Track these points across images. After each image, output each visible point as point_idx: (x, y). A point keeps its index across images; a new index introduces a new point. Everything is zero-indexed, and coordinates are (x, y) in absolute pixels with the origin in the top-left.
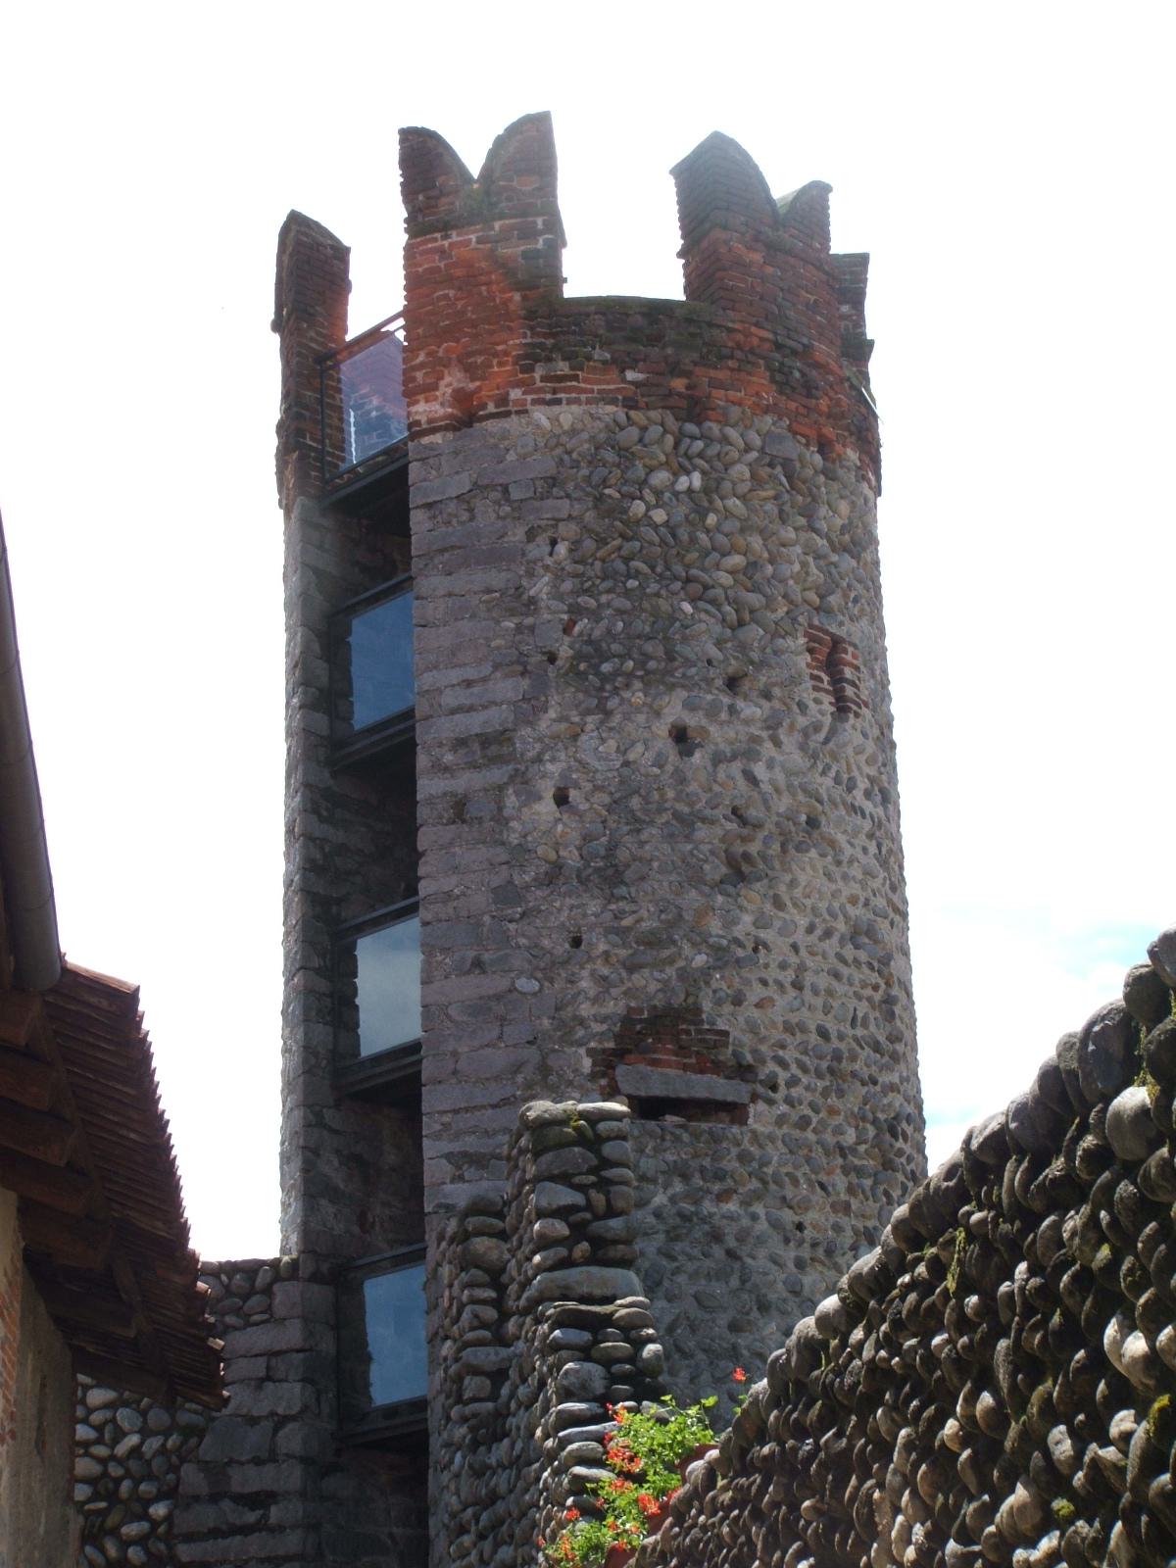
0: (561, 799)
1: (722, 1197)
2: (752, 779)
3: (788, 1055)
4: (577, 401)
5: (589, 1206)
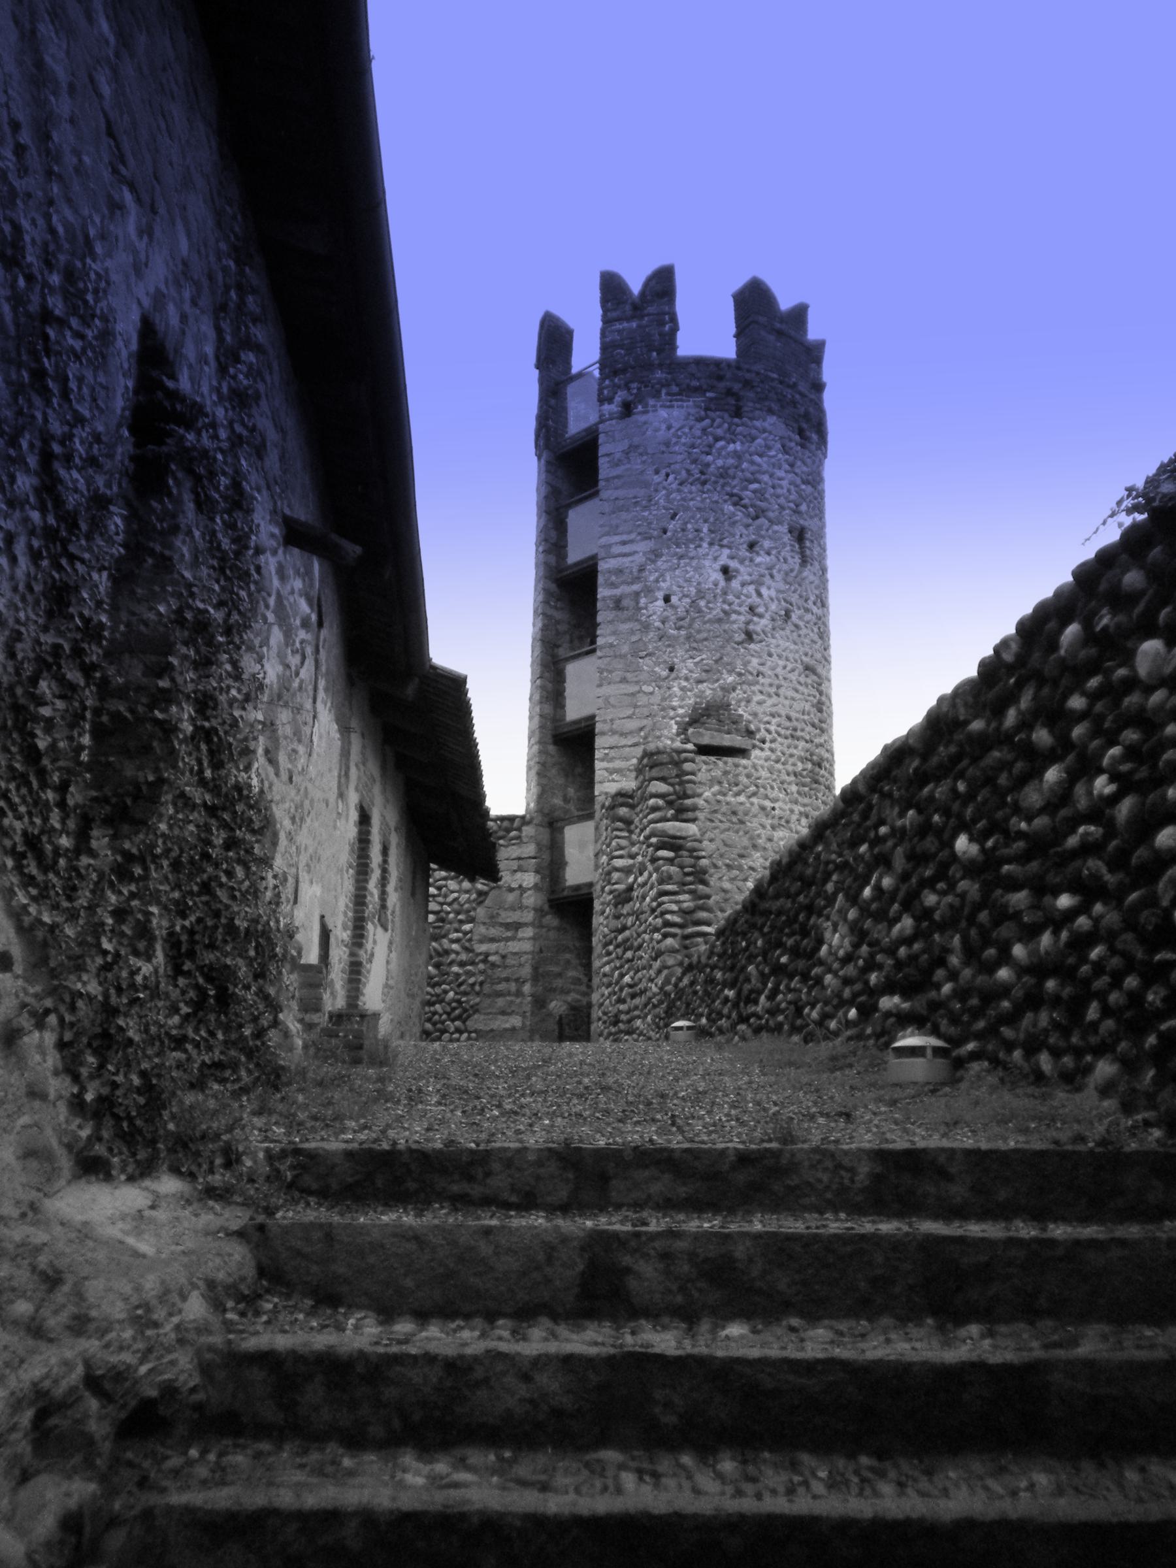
0: (667, 599)
1: (738, 794)
2: (759, 595)
3: (772, 728)
4: (682, 407)
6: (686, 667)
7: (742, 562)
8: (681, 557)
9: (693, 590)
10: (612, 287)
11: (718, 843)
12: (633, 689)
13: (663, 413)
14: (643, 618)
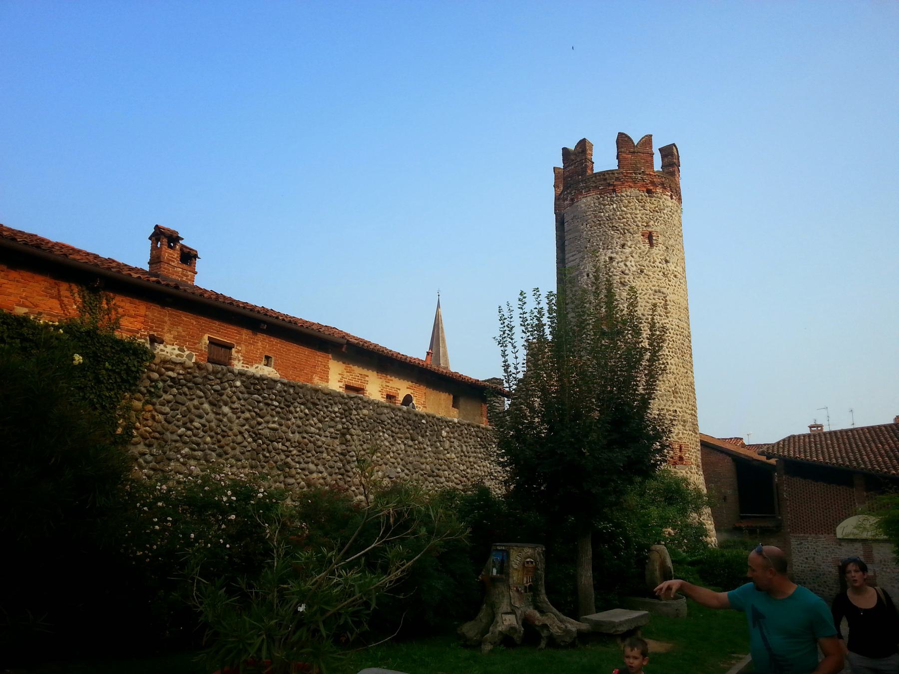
0: (588, 275)
2: (626, 265)
4: (590, 196)
7: (617, 253)
14: (580, 285)
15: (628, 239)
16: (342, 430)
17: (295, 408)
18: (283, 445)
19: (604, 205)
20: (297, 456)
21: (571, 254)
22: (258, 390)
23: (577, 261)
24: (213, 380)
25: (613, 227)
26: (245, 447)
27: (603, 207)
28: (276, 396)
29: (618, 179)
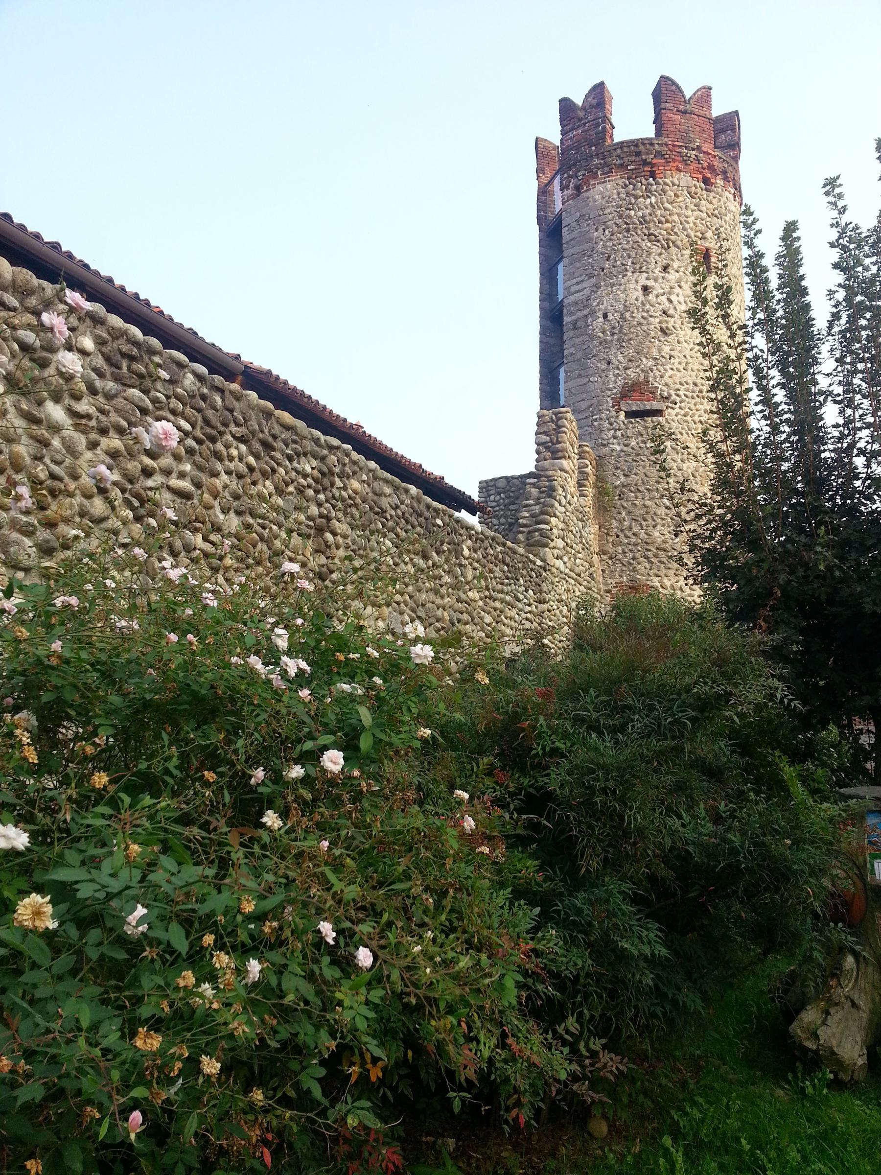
0: (605, 316)
2: (670, 301)
3: (681, 393)
5: (551, 441)
6: (618, 359)
7: (656, 280)
8: (612, 285)
9: (621, 306)
10: (566, 106)
11: (642, 475)
12: (585, 381)
13: (600, 188)
15: (674, 257)
16: (319, 521)
17: (227, 446)
18: (205, 539)
19: (636, 197)
20: (236, 570)
21: (575, 281)
22: (141, 376)
23: (587, 292)
24: (15, 309)
25: (650, 235)
26: (116, 533)
27: (633, 201)
28: (184, 405)
29: (659, 154)
